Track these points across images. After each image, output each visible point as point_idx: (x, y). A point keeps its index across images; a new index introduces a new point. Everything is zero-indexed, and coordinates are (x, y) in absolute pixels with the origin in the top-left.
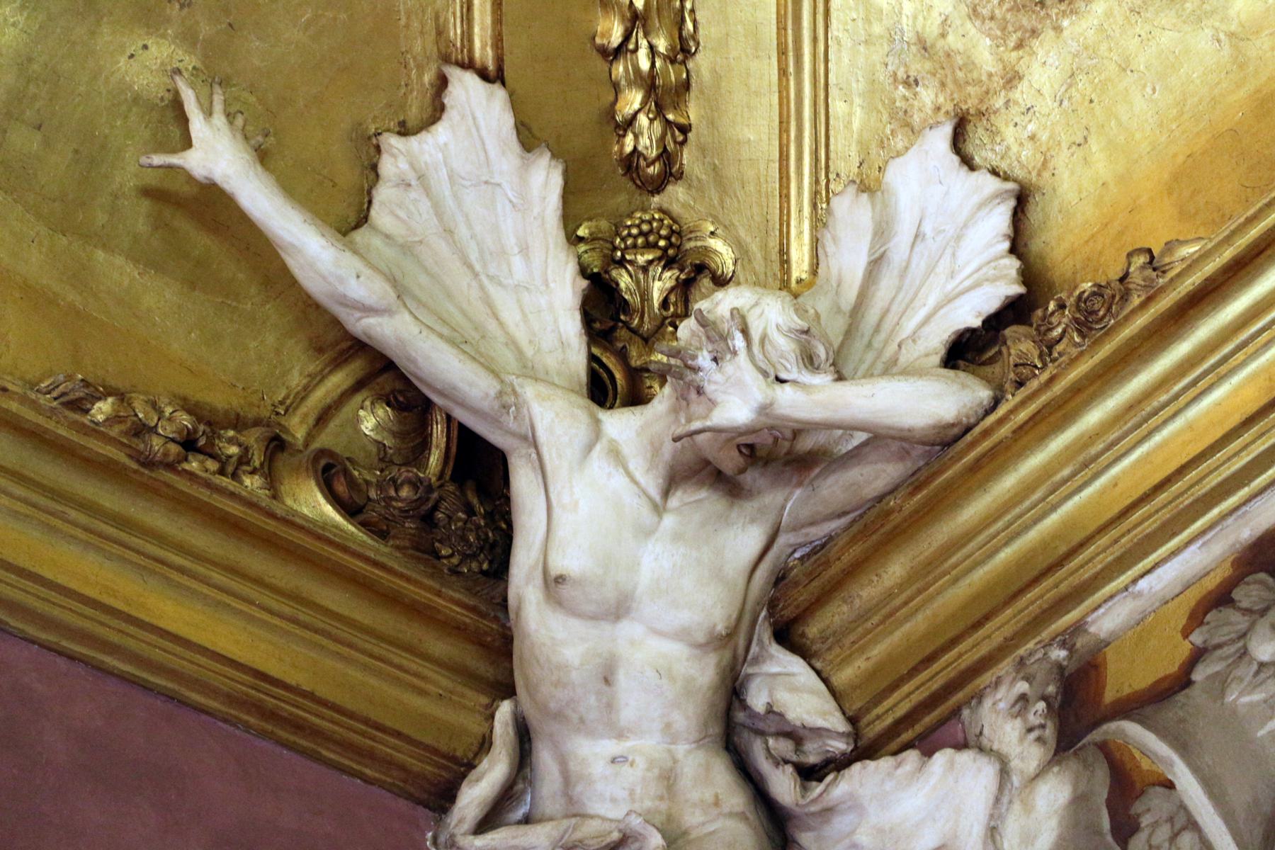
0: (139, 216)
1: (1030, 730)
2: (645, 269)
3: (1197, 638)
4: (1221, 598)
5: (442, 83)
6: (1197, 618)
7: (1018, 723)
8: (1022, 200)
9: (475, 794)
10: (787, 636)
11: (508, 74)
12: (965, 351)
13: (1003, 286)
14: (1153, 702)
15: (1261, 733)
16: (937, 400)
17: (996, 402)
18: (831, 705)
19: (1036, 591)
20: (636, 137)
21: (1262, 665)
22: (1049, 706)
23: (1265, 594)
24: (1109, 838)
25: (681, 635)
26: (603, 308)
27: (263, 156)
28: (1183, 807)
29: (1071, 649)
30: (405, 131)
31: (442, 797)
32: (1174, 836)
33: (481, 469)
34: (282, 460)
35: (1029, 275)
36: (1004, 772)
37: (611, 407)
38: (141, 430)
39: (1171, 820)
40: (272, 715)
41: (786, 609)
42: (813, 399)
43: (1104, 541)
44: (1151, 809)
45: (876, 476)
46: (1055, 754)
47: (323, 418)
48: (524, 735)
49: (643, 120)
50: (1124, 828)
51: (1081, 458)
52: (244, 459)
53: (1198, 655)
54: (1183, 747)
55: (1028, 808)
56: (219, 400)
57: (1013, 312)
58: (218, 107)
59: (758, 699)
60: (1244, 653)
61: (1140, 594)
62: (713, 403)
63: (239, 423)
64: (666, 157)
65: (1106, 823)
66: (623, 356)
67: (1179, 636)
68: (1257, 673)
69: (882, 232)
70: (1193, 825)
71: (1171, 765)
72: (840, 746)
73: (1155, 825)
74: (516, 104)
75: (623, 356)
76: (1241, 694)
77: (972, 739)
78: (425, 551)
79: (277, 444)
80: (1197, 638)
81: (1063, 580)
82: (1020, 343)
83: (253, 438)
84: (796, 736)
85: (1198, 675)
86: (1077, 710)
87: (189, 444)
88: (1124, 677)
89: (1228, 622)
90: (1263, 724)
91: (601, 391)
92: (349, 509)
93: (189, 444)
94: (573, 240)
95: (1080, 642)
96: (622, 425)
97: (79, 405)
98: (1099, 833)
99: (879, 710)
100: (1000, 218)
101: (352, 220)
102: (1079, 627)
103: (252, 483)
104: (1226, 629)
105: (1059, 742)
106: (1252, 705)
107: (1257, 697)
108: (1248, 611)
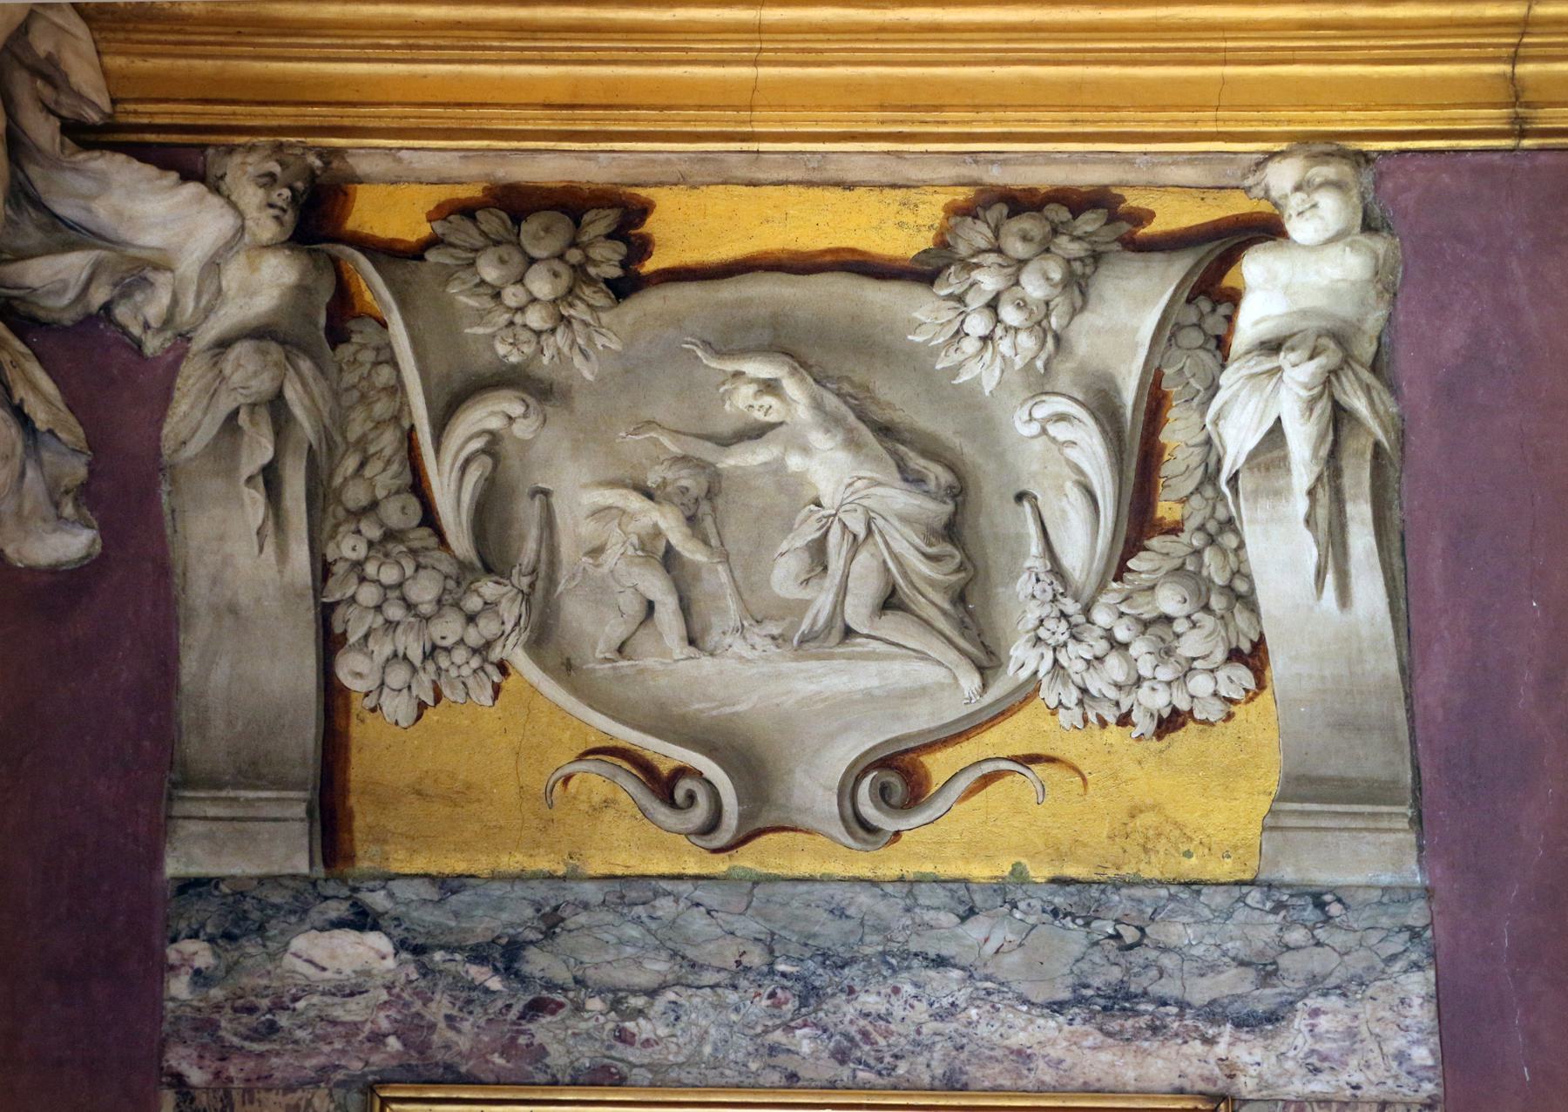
1: (271, 206)
4: (467, 210)
6: (442, 212)
7: (261, 192)
14: (387, 253)
15: (468, 331)
18: (101, 83)
19: (324, 110)
21: (483, 282)
22: (293, 196)
23: (501, 230)
24: (322, 334)
28: (389, 346)
29: (327, 164)
32: (376, 364)
39: (378, 349)
43: (398, 110)
44: (363, 334)
46: (290, 239)
50: (337, 335)
51: (411, 41)
53: (434, 242)
54: (404, 304)
55: (253, 268)
60: (472, 264)
61: (400, 160)
65: (322, 321)
67: (424, 217)
68: (477, 285)
70: (394, 363)
71: (390, 311)
73: (363, 346)
76: (461, 292)
77: (211, 179)
80: (440, 228)
81: (349, 116)
85: (432, 256)
90: (471, 326)
95: (335, 164)
98: (316, 325)
99: (141, 108)
104: (463, 236)
105: (295, 232)
106: (467, 306)
107: (473, 302)
108: (484, 234)
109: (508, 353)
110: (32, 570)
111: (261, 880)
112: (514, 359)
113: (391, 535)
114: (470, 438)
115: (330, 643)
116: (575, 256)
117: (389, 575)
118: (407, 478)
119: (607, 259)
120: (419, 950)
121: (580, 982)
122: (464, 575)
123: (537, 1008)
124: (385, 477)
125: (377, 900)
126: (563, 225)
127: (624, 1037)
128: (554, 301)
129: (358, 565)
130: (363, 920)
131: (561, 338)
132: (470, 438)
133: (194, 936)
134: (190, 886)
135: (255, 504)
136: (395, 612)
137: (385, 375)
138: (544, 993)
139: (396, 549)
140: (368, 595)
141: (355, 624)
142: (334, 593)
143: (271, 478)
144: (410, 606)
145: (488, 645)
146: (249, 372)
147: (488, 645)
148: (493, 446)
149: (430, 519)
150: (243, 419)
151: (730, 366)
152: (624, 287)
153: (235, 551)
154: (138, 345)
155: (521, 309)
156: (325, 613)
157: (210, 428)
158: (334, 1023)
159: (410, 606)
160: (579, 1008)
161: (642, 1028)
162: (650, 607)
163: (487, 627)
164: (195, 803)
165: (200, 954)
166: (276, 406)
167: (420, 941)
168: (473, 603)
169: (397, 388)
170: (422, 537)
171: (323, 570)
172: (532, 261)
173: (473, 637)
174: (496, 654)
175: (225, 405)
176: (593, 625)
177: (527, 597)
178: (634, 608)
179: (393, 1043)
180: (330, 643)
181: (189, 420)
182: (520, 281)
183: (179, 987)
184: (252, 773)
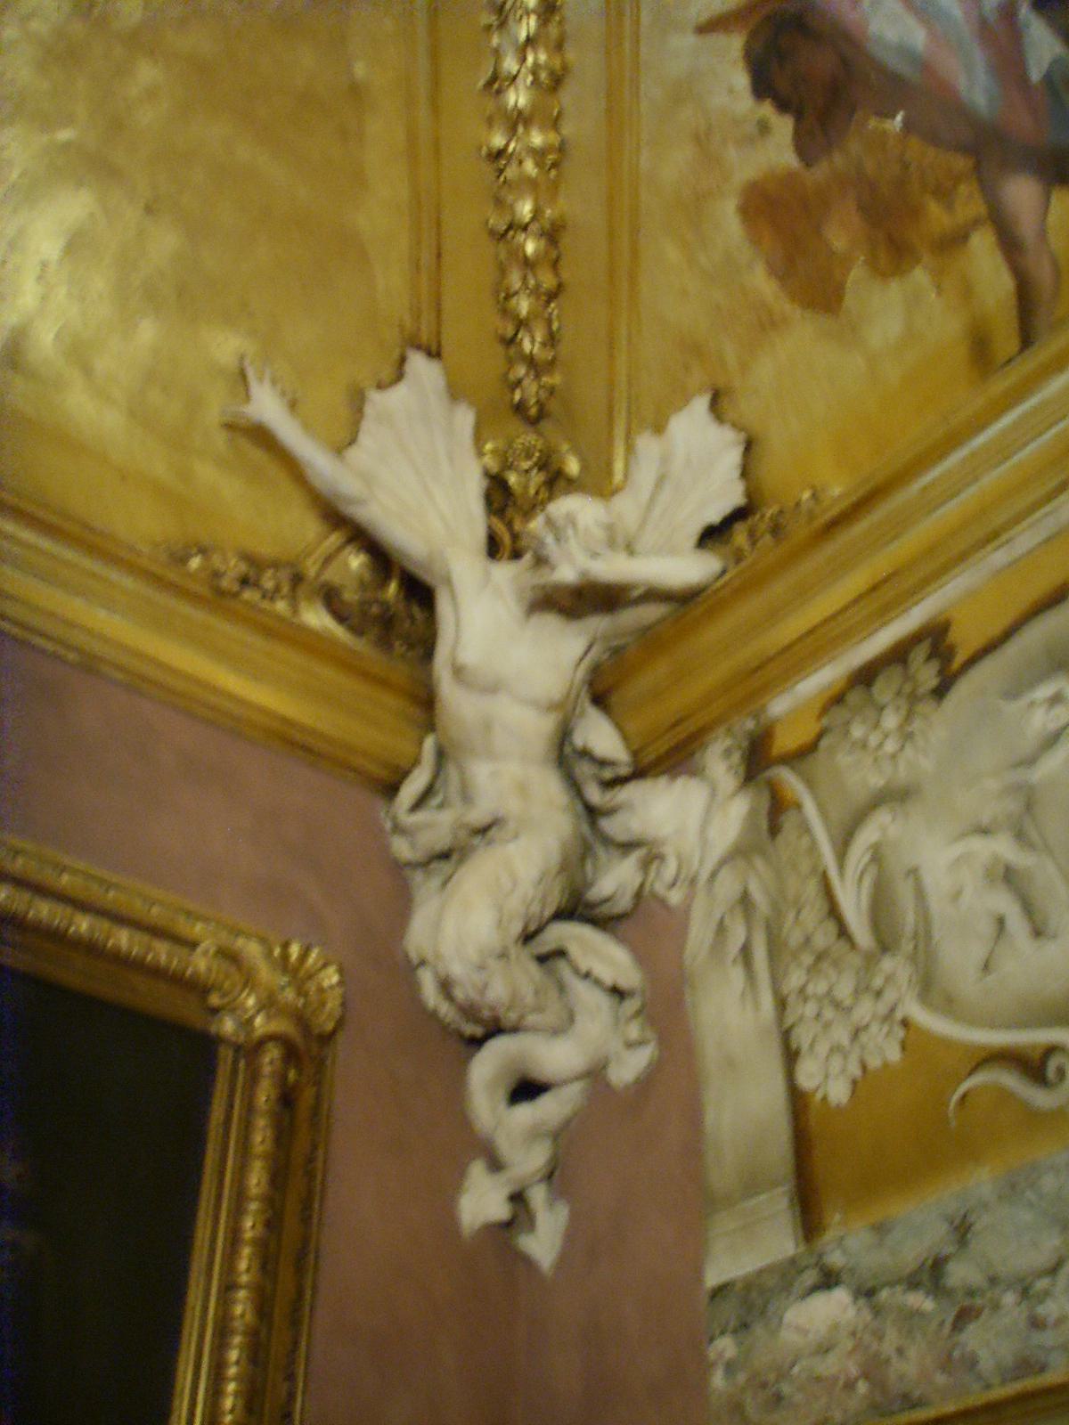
0: (220, 439)
2: (527, 471)
3: (825, 721)
4: (838, 699)
5: (403, 360)
8: (749, 446)
9: (411, 789)
10: (600, 699)
11: (446, 351)
12: (711, 536)
13: (734, 497)
16: (687, 568)
17: (724, 572)
20: (523, 391)
25: (535, 704)
26: (499, 496)
27: (293, 405)
30: (381, 386)
31: (391, 790)
33: (420, 593)
34: (302, 590)
35: (749, 494)
36: (713, 793)
37: (498, 560)
38: (217, 575)
40: (292, 743)
41: (601, 690)
42: (613, 568)
44: (789, 822)
45: (650, 613)
46: (745, 780)
47: (328, 560)
48: (441, 755)
49: (526, 383)
50: (774, 830)
52: (277, 589)
54: (810, 783)
56: (266, 550)
57: (739, 515)
58: (267, 376)
59: (579, 740)
62: (553, 568)
63: (275, 565)
64: (541, 405)
66: (509, 525)
69: (665, 460)
72: (624, 771)
74: (448, 373)
75: (509, 525)
78: (384, 642)
79: (297, 579)
82: (740, 535)
83: (284, 575)
84: (603, 763)
86: (757, 759)
87: (245, 581)
88: (786, 741)
89: (840, 714)
91: (493, 548)
92: (340, 618)
93: (245, 581)
94: (480, 453)
96: (504, 572)
97: (183, 560)
100: (734, 457)
101: (347, 441)
102: (763, 708)
103: (281, 606)
109: (876, 781)
110: (627, 1087)
111: (760, 1272)
112: (881, 782)
113: (820, 957)
114: (863, 856)
115: (791, 1057)
116: (908, 688)
117: (819, 987)
118: (826, 908)
119: (927, 675)
120: (870, 1293)
121: (993, 1281)
122: (871, 961)
123: (964, 1317)
124: (812, 913)
125: (836, 1259)
126: (895, 672)
127: (1036, 1324)
128: (901, 727)
129: (802, 990)
130: (829, 1280)
131: (909, 751)
132: (863, 856)
133: (722, 1333)
134: (720, 1292)
135: (737, 975)
136: (829, 1013)
137: (805, 841)
138: (967, 1302)
139: (825, 965)
140: (810, 1009)
141: (802, 1037)
142: (790, 1019)
143: (746, 952)
144: (837, 1005)
145: (893, 1010)
146: (728, 886)
147: (893, 1010)
148: (877, 855)
149: (843, 932)
150: (727, 921)
151: (1022, 702)
152: (940, 692)
153: (730, 1014)
154: (663, 902)
155: (880, 745)
156: (786, 1035)
157: (709, 935)
158: (818, 1379)
159: (837, 1005)
160: (996, 1306)
161: (1050, 1309)
162: (1001, 922)
163: (890, 996)
164: (723, 1225)
165: (725, 1346)
166: (745, 901)
167: (870, 1284)
168: (878, 982)
169: (813, 848)
170: (842, 946)
171: (781, 1004)
172: (882, 709)
173: (882, 1008)
174: (899, 1015)
175: (718, 916)
176: (959, 958)
177: (913, 958)
178: (986, 928)
179: (862, 1387)
180: (791, 1057)
181: (699, 934)
182: (877, 725)
183: (718, 1380)
184: (752, 1185)
